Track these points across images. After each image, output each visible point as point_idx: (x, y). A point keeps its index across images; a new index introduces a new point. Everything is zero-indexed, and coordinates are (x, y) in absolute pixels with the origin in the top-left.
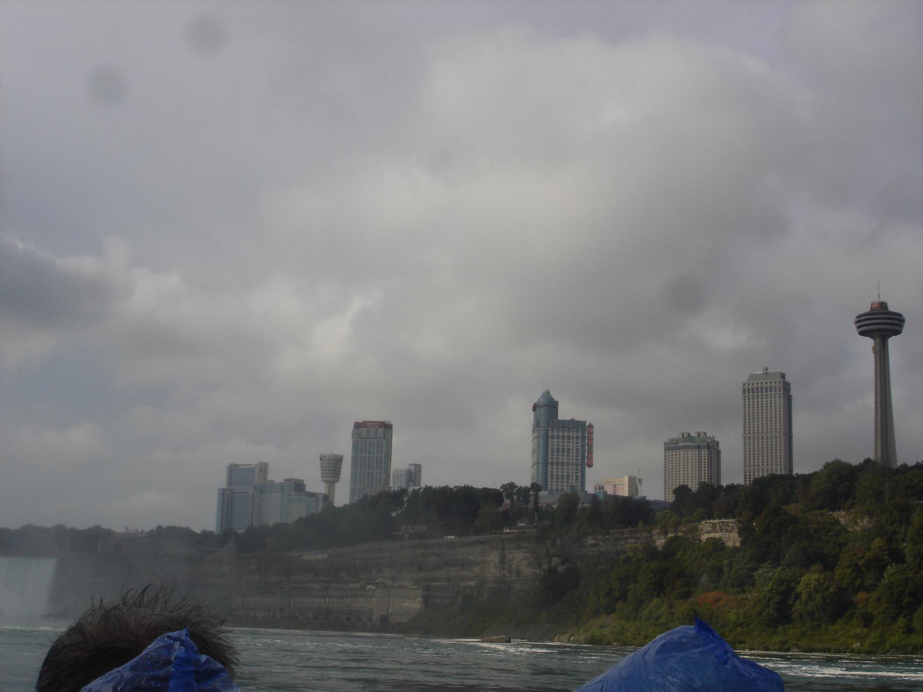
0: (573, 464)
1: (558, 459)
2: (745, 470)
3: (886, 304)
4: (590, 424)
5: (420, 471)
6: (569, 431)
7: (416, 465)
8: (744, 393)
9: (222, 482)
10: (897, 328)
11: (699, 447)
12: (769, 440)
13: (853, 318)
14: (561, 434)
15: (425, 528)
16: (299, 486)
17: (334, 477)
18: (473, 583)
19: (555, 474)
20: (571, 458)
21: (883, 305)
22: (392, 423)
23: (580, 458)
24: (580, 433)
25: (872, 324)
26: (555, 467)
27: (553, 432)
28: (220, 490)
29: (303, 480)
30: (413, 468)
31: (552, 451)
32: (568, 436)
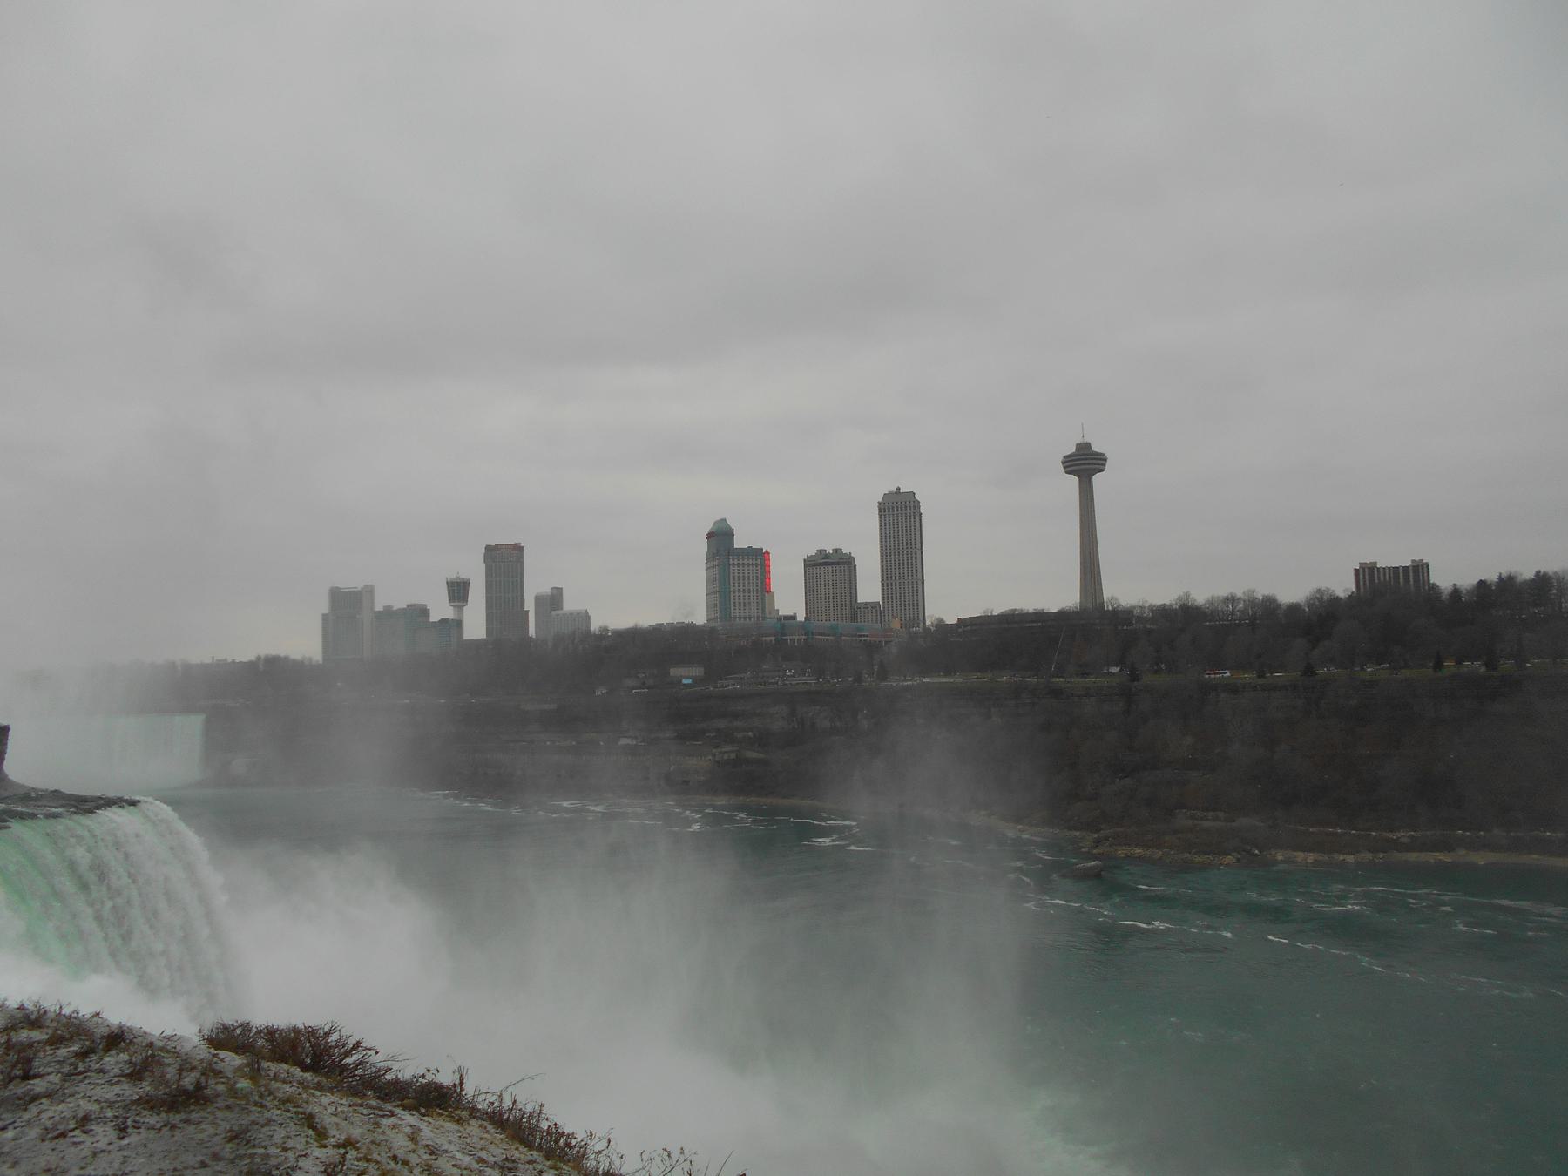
0: (753, 591)
3: (1090, 444)
4: (767, 551)
6: (748, 559)
8: (880, 511)
9: (324, 608)
10: (1102, 467)
11: (838, 563)
12: (905, 556)
13: (1061, 459)
14: (741, 562)
16: (424, 611)
18: (750, 734)
21: (1088, 446)
22: (522, 545)
27: (733, 560)
28: (323, 615)
29: (425, 605)
30: (555, 592)
31: (734, 579)
32: (748, 564)
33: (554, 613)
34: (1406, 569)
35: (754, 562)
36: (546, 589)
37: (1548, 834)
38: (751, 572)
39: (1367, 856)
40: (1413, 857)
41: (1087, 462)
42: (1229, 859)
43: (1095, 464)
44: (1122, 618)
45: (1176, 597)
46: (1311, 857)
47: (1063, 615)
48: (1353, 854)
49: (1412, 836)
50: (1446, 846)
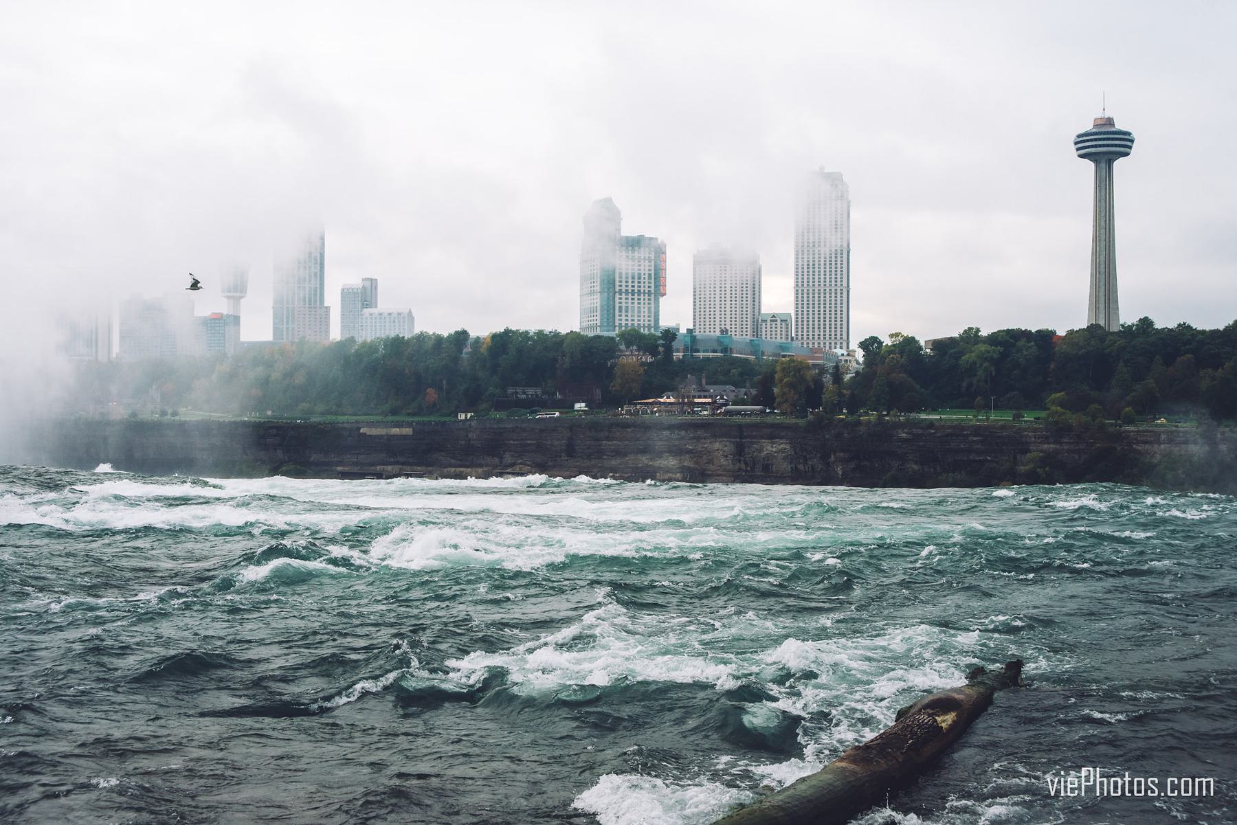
1: (627, 286)
2: (797, 290)
5: (376, 288)
7: (372, 280)
10: (1127, 150)
13: (1073, 138)
15: (539, 391)
17: (241, 292)
19: (624, 305)
20: (642, 285)
21: (1110, 122)
23: (653, 285)
24: (653, 253)
25: (1104, 146)
26: (624, 296)
30: (368, 284)
33: (367, 311)
35: (647, 256)
36: (355, 280)
38: (642, 268)
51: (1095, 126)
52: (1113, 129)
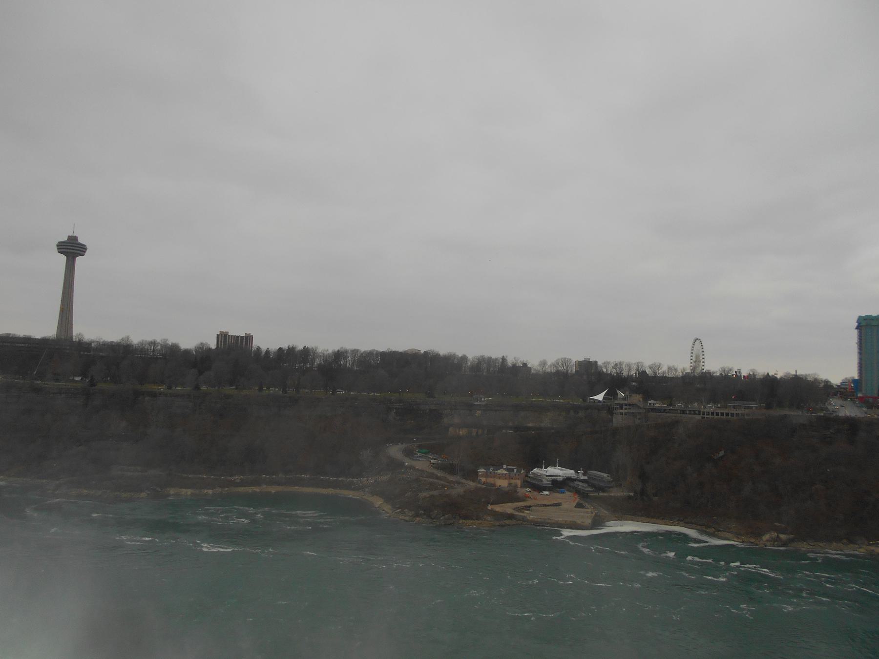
3: (77, 237)
13: (56, 243)
21: (76, 238)
34: (242, 337)
37: (303, 476)
39: (219, 490)
40: (241, 489)
41: (73, 248)
42: (143, 495)
43: (77, 250)
44: (83, 347)
45: (121, 338)
46: (189, 492)
47: (44, 341)
48: (213, 489)
49: (241, 479)
50: (257, 483)
51: (68, 239)
52: (77, 242)
